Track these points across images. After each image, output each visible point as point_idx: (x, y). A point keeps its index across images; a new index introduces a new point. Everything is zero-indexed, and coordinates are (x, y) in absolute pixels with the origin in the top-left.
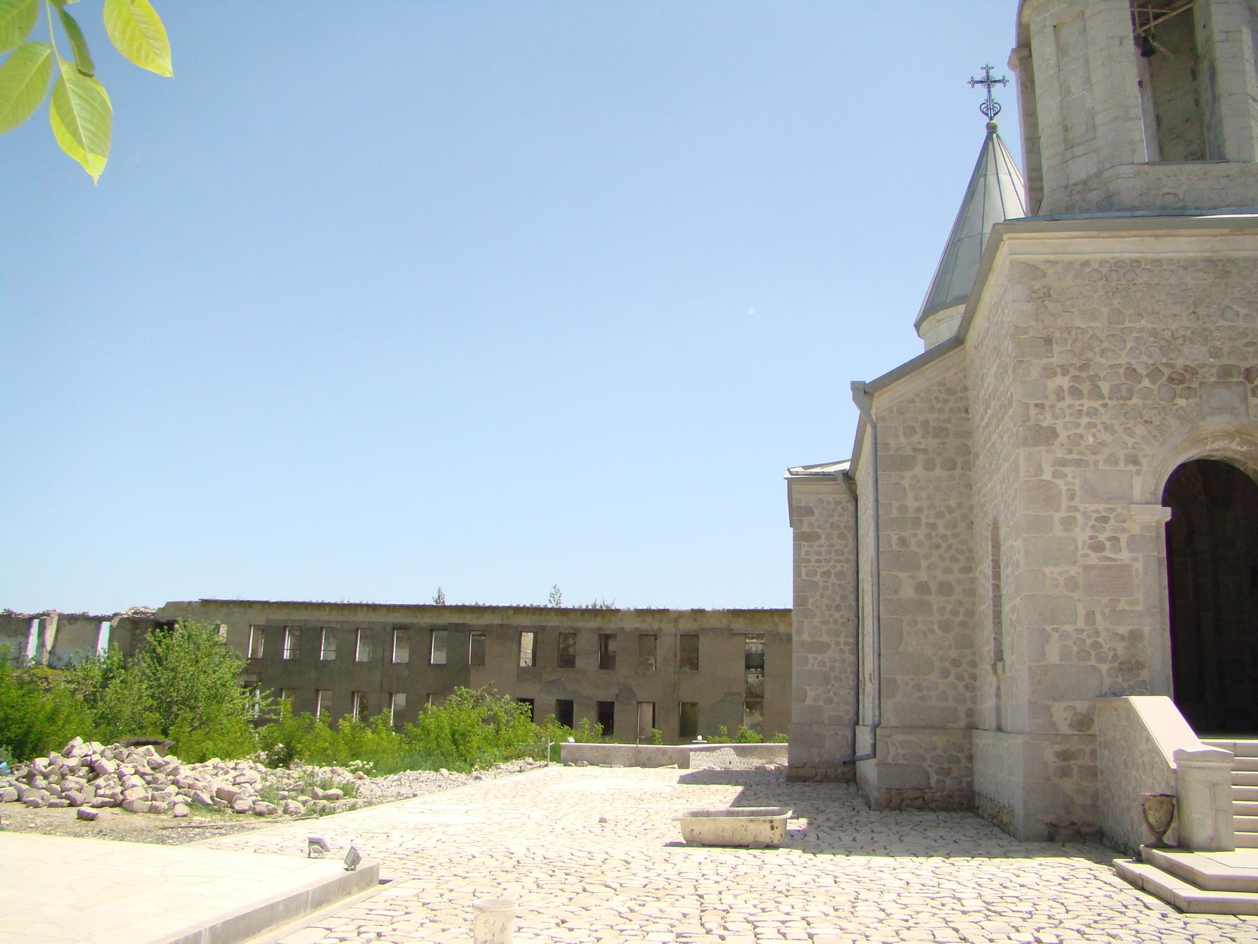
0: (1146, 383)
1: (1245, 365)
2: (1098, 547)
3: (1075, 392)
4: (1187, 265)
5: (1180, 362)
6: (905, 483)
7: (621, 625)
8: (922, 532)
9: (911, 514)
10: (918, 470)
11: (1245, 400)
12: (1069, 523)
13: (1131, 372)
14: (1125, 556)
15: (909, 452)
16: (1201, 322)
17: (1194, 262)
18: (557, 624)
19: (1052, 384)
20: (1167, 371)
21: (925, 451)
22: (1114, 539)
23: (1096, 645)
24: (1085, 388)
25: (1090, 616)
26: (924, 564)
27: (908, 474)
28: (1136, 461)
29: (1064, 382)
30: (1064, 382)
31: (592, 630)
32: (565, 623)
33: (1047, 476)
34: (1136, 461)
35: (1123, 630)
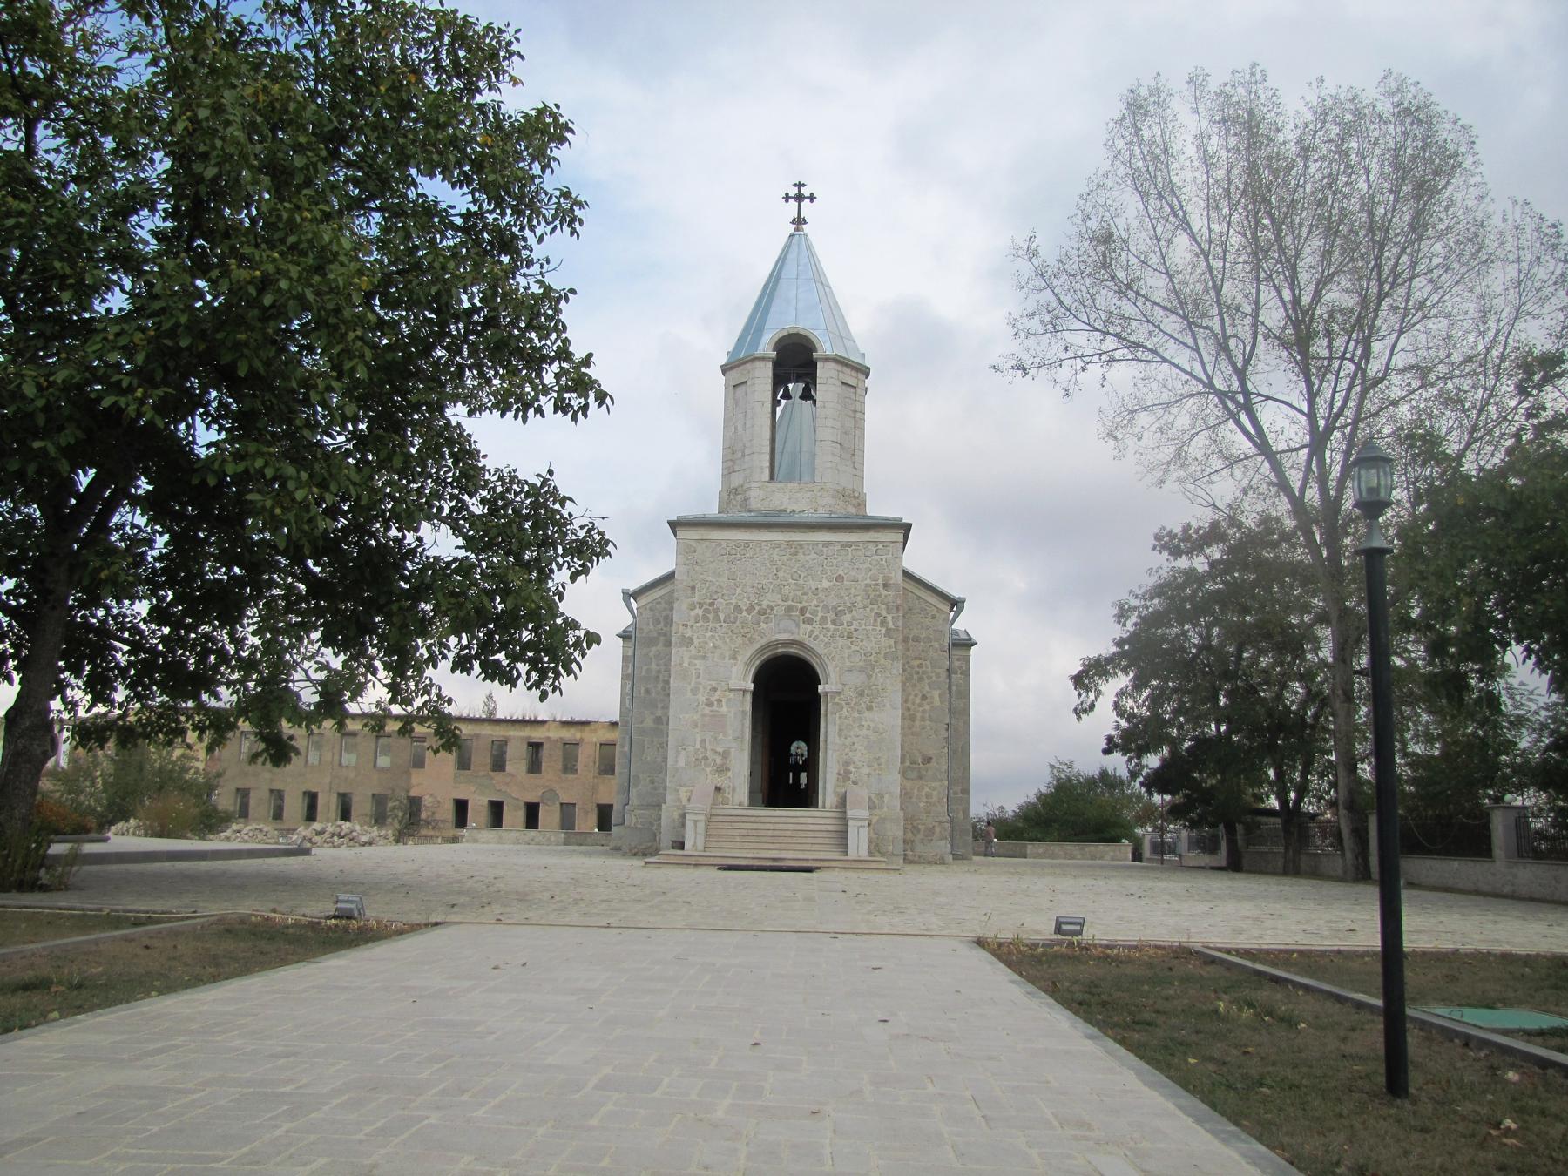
0: (745, 613)
1: (800, 606)
2: (710, 704)
3: (705, 618)
4: (775, 545)
5: (765, 603)
6: (652, 654)
7: (547, 734)
8: (660, 686)
9: (654, 674)
10: (660, 647)
11: (798, 626)
12: (695, 691)
13: (737, 608)
14: (724, 709)
15: (655, 635)
16: (778, 582)
17: (779, 546)
18: (489, 732)
19: (693, 613)
20: (757, 608)
21: (665, 635)
22: (719, 701)
23: (706, 758)
24: (711, 616)
25: (703, 741)
26: (660, 706)
27: (654, 649)
28: (734, 657)
29: (699, 612)
30: (699, 612)
31: (522, 738)
32: (498, 732)
33: (686, 664)
34: (734, 657)
35: (720, 750)
